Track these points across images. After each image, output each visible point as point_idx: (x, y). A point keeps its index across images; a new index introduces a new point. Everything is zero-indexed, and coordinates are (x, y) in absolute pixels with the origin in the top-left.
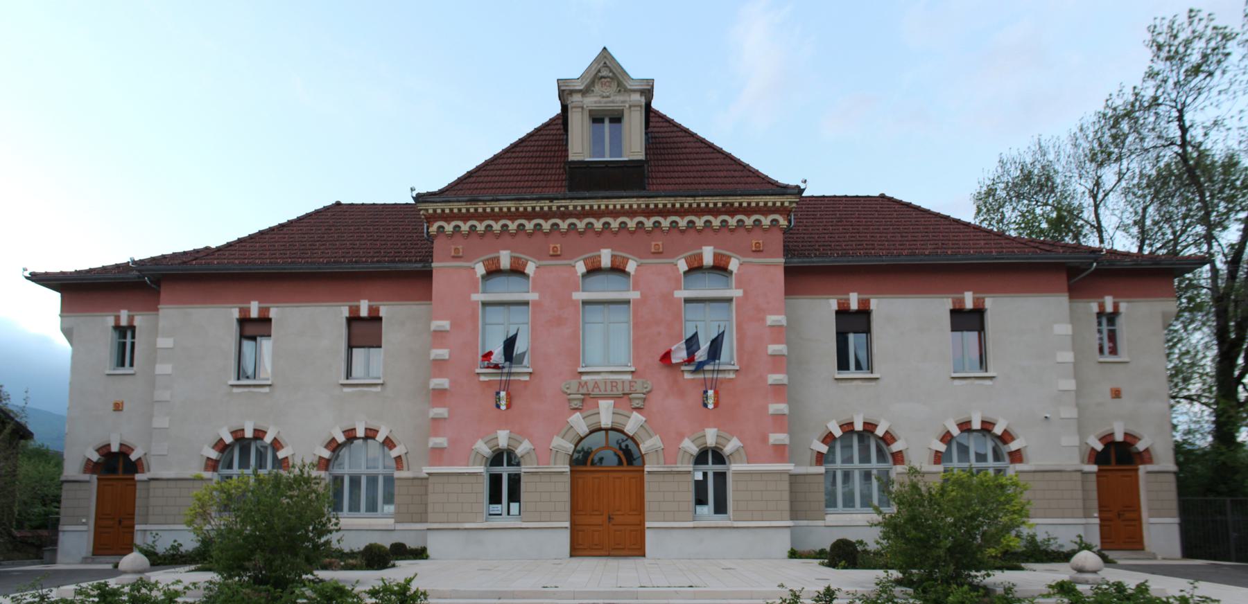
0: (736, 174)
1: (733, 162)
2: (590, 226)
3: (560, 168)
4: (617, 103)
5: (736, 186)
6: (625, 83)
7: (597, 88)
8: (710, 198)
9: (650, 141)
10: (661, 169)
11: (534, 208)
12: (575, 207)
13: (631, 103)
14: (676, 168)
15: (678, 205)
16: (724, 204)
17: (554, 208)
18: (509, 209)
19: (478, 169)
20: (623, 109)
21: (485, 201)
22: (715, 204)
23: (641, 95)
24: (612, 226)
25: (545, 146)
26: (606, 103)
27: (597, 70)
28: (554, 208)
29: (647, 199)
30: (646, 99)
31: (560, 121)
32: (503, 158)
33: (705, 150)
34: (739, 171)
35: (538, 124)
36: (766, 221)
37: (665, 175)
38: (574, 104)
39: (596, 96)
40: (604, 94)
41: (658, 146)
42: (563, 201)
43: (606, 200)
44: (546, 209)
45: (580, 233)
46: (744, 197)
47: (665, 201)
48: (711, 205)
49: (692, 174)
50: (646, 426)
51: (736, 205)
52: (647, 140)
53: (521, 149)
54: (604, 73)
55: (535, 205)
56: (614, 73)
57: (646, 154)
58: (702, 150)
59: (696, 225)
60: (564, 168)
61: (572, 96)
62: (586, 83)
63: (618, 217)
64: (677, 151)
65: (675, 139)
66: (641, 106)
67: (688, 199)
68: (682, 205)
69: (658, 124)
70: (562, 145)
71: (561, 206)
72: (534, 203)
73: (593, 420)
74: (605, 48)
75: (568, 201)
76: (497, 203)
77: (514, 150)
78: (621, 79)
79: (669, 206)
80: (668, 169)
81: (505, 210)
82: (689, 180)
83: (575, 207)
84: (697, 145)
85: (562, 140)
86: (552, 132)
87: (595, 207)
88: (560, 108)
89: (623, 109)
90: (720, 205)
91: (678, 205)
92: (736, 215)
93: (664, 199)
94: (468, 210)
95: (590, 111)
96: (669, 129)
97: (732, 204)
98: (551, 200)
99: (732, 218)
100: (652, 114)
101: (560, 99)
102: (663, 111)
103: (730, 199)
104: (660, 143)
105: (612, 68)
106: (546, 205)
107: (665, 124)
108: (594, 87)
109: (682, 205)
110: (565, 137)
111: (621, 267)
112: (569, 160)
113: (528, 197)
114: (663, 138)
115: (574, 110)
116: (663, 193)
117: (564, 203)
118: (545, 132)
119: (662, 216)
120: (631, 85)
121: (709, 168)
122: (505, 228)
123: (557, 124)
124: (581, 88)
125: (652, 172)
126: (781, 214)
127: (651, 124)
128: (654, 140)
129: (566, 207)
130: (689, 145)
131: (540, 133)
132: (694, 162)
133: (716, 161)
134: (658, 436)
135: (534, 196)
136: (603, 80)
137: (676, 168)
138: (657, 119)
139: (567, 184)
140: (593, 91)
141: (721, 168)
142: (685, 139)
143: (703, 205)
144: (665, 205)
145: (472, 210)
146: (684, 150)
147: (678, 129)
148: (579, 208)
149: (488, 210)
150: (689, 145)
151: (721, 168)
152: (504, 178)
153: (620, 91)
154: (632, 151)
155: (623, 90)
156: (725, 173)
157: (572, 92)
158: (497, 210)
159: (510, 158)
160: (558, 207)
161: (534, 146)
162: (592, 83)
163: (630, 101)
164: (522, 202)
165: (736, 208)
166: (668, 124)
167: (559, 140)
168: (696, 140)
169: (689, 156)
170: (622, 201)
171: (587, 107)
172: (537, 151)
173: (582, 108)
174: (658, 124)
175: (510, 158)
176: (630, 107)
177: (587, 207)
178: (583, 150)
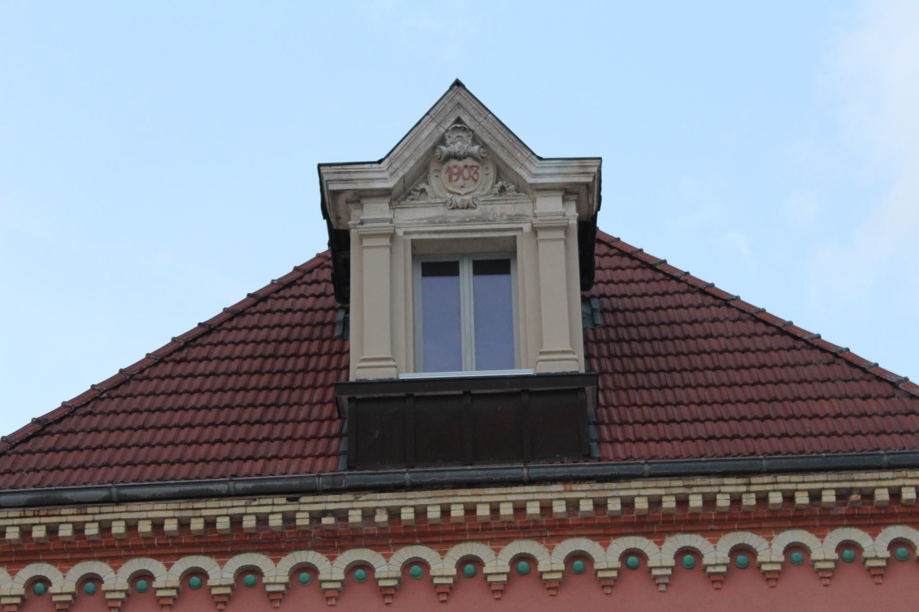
0: (872, 406)
1: (857, 373)
2: (416, 569)
3: (322, 402)
4: (493, 221)
5: (875, 440)
6: (518, 170)
7: (436, 184)
8: (795, 478)
9: (599, 320)
10: (635, 396)
11: (236, 521)
12: (369, 514)
13: (536, 221)
14: (681, 395)
15: (696, 502)
16: (842, 495)
17: (302, 520)
18: (158, 525)
19: (70, 410)
20: (515, 237)
21: (81, 504)
22: (815, 496)
23: (565, 200)
24: (486, 570)
25: (278, 342)
26: (462, 222)
27: (437, 136)
28: (302, 520)
29: (597, 486)
30: (578, 210)
31: (327, 274)
32: (149, 378)
33: (768, 341)
34: (879, 396)
35: (259, 282)
37: (649, 413)
38: (369, 227)
39: (435, 205)
40: (458, 199)
41: (623, 333)
42: (330, 498)
43: (469, 492)
44: (276, 521)
45: (386, 593)
46: (903, 473)
47: (654, 488)
48: (802, 499)
49: (732, 410)
51: (882, 495)
52: (589, 317)
53: (204, 352)
54: (457, 145)
55: (241, 510)
56: (484, 145)
57: (588, 357)
58: (759, 342)
59: (760, 559)
60: (336, 402)
61: (362, 207)
62: (401, 174)
63: (508, 540)
64: (682, 346)
65: (674, 314)
66: (566, 229)
67: (727, 481)
68: (710, 501)
69: (619, 275)
70: (332, 339)
71: (325, 513)
72: (237, 507)
74: (458, 83)
75: (345, 497)
76: (122, 508)
77: (183, 354)
78: (510, 162)
79: (669, 503)
80: (657, 395)
81: (145, 528)
82: (725, 428)
83: (369, 514)
84: (742, 327)
85: (333, 324)
86: (300, 303)
87: (434, 513)
88: (326, 238)
89: (515, 237)
90: (829, 497)
91: (696, 502)
92: (886, 525)
93: (651, 484)
94: (26, 532)
95: (414, 243)
96: (654, 287)
97: (868, 495)
98: (293, 494)
99: (874, 535)
100: (599, 249)
101: (326, 215)
102: (632, 238)
103: (862, 480)
104: (629, 325)
105: (478, 131)
107: (639, 274)
108: (427, 181)
109: (710, 501)
110: (341, 315)
112: (352, 379)
113: (222, 488)
114: (635, 310)
115: (366, 243)
116: (647, 468)
117: (332, 502)
118: (279, 304)
119: (648, 535)
120: (535, 175)
121: (783, 390)
122: (142, 584)
123: (317, 282)
124: (389, 185)
125: (608, 406)
127: (599, 275)
128: (610, 319)
129: (341, 515)
130: (719, 328)
131: (262, 307)
132: (736, 377)
133: (805, 372)
135: (240, 486)
136: (453, 162)
137: (681, 395)
138: (616, 261)
139: (343, 448)
140: (423, 191)
141: (822, 389)
142: (704, 313)
143: (776, 498)
144: (655, 502)
145: (39, 533)
146: (704, 344)
147: (683, 287)
148: (381, 518)
149: (92, 530)
150: (719, 328)
151: (822, 389)
152: (147, 436)
153: (503, 189)
154: (544, 350)
155: (512, 187)
156: (838, 406)
157: (360, 197)
158: (118, 528)
159: (170, 377)
160: (316, 517)
161: (244, 342)
162: (423, 171)
163: (535, 216)
164: (197, 505)
165: (881, 506)
166: (649, 274)
167: (323, 324)
168: (736, 314)
169: (721, 360)
170: (518, 493)
171: (405, 233)
172: (252, 357)
173: (392, 237)
174: (619, 275)
175: (170, 377)
176: (535, 230)
177: (407, 515)
178: (392, 352)
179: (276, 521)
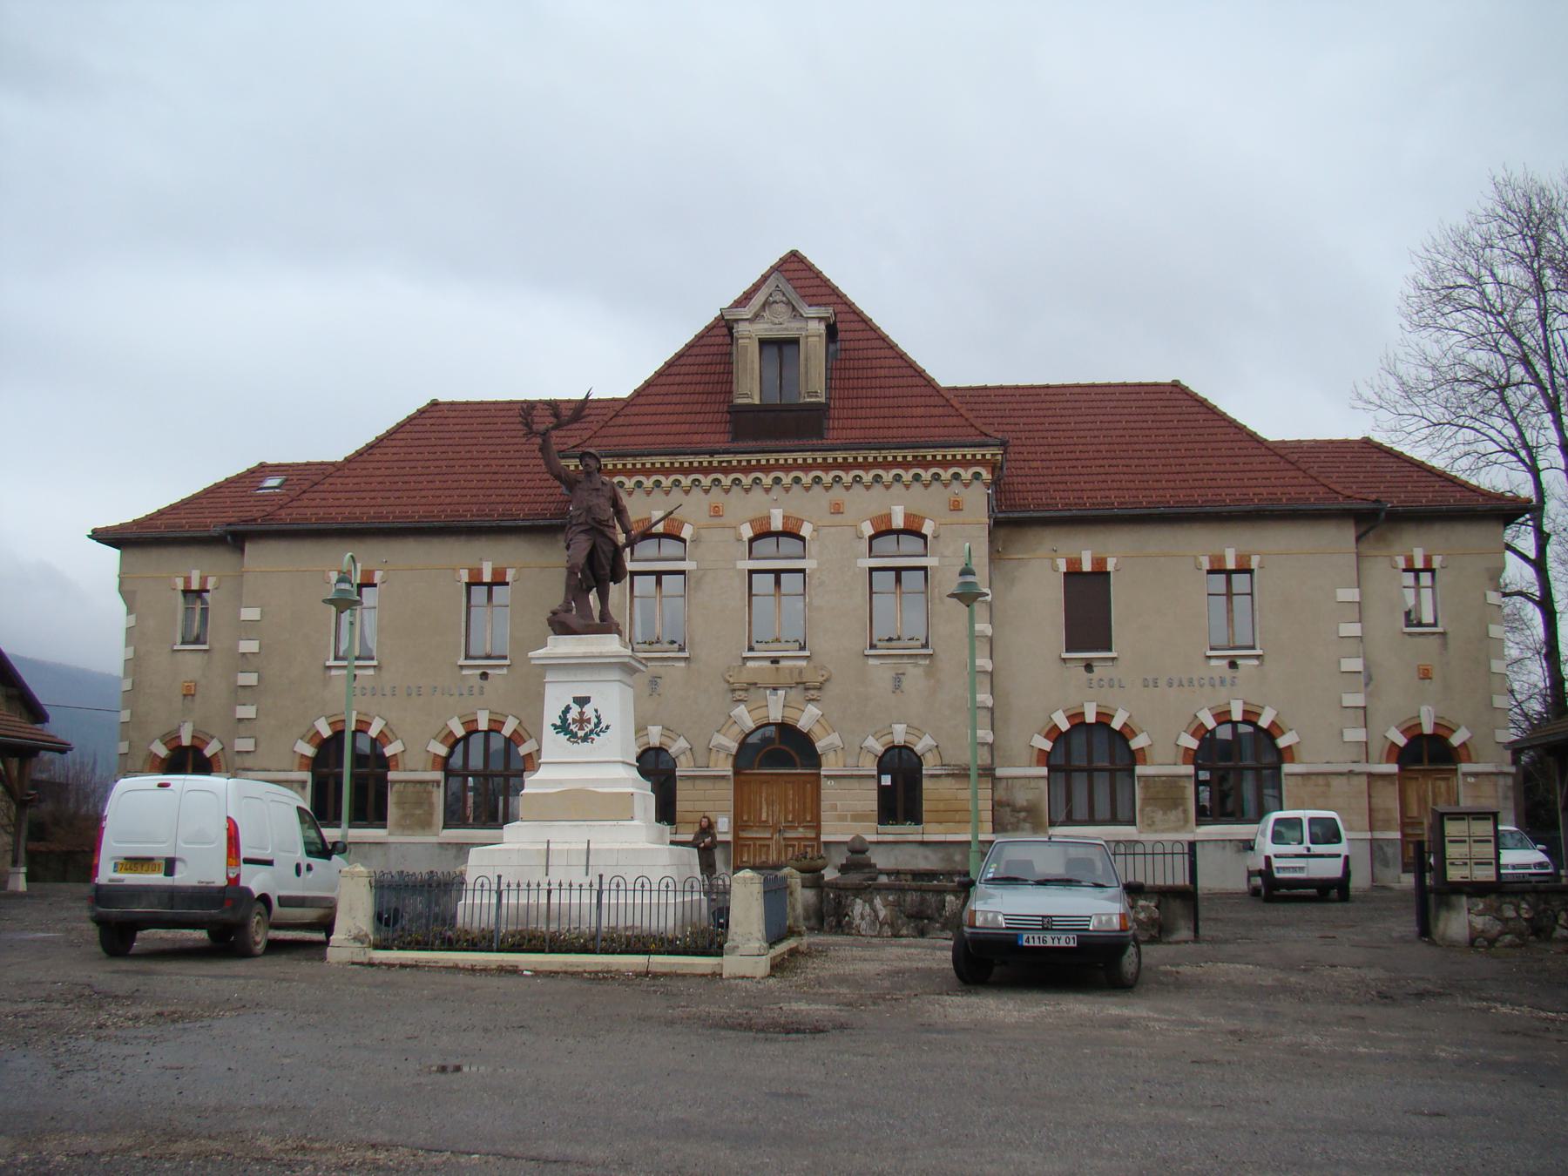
28: (715, 464)
36: (966, 474)
50: (823, 721)
68: (865, 458)
71: (723, 462)
72: (691, 458)
73: (761, 713)
97: (925, 457)
98: (712, 454)
103: (922, 452)
106: (705, 459)
109: (865, 458)
111: (795, 531)
126: (983, 467)
129: (730, 462)
134: (837, 734)
179: (705, 464)
